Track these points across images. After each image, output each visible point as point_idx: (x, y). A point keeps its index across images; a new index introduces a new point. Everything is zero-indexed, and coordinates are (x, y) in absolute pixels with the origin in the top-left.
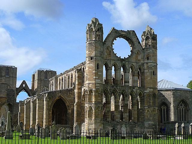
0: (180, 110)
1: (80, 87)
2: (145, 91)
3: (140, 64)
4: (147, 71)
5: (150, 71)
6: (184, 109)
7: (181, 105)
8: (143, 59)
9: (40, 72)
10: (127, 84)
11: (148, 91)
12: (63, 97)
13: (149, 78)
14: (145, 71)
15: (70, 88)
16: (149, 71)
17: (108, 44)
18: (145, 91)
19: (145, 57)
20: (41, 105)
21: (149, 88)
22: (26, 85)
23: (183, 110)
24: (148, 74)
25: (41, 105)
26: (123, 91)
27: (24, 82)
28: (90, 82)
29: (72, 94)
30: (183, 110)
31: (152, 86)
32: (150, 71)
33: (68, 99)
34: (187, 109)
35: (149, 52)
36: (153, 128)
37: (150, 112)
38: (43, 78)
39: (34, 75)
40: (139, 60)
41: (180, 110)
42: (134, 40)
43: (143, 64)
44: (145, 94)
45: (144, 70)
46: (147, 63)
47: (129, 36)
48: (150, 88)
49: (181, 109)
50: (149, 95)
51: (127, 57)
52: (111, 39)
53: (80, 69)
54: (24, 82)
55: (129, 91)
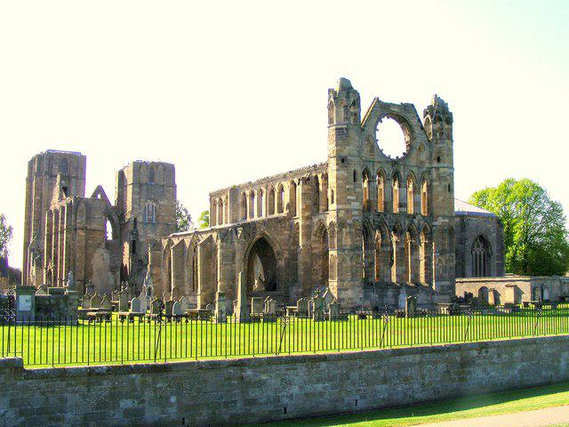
0: (476, 255)
1: (307, 214)
2: (435, 223)
3: (424, 169)
4: (438, 183)
5: (443, 183)
6: (482, 253)
7: (478, 246)
8: (430, 158)
9: (138, 166)
10: (403, 209)
11: (440, 222)
13: (441, 198)
15: (276, 215)
17: (369, 130)
18: (435, 223)
19: (434, 156)
22: (104, 195)
23: (480, 255)
24: (440, 189)
26: (396, 223)
27: (100, 190)
28: (340, 207)
29: (285, 227)
30: (480, 255)
31: (446, 213)
32: (443, 183)
33: (279, 238)
34: (488, 253)
36: (449, 294)
38: (145, 180)
39: (121, 175)
40: (422, 162)
41: (476, 255)
42: (413, 122)
43: (429, 171)
46: (437, 169)
47: (403, 115)
48: (444, 217)
49: (478, 253)
50: (443, 231)
51: (401, 156)
52: (374, 120)
53: (308, 179)
54: (100, 190)
55: (407, 222)
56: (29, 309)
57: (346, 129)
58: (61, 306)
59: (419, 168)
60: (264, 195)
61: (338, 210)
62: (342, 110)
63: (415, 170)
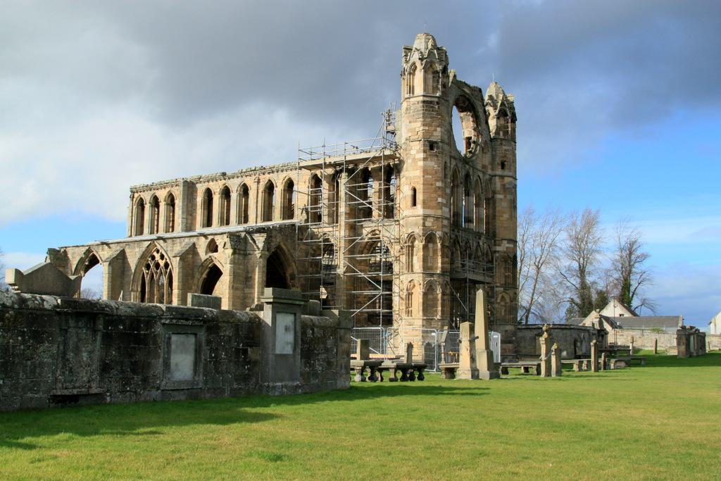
2: (498, 248)
12: (284, 247)
14: (499, 196)
16: (505, 197)
18: (498, 248)
19: (498, 160)
20: (239, 269)
21: (505, 242)
25: (239, 269)
28: (429, 212)
35: (505, 150)
37: (508, 301)
44: (497, 255)
45: (494, 192)
46: (502, 177)
56: (288, 350)
57: (438, 103)
58: (330, 343)
59: (484, 173)
60: (252, 194)
61: (425, 217)
62: (430, 76)
63: (481, 175)
